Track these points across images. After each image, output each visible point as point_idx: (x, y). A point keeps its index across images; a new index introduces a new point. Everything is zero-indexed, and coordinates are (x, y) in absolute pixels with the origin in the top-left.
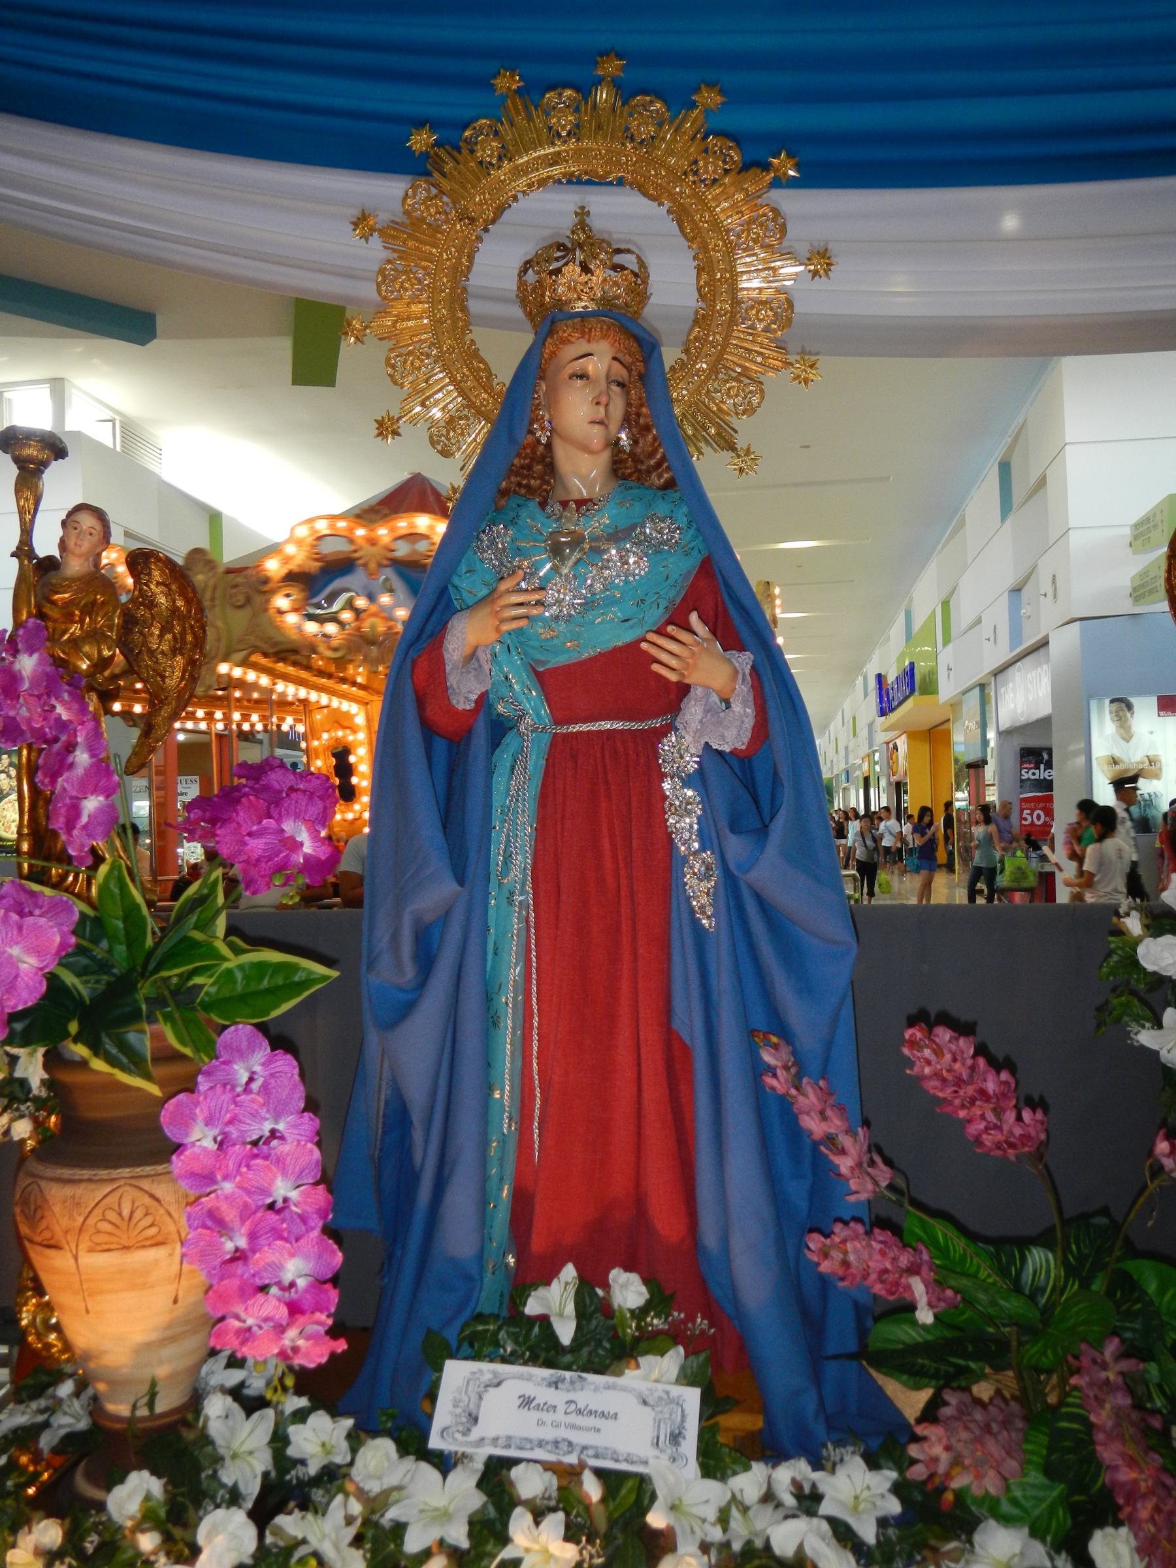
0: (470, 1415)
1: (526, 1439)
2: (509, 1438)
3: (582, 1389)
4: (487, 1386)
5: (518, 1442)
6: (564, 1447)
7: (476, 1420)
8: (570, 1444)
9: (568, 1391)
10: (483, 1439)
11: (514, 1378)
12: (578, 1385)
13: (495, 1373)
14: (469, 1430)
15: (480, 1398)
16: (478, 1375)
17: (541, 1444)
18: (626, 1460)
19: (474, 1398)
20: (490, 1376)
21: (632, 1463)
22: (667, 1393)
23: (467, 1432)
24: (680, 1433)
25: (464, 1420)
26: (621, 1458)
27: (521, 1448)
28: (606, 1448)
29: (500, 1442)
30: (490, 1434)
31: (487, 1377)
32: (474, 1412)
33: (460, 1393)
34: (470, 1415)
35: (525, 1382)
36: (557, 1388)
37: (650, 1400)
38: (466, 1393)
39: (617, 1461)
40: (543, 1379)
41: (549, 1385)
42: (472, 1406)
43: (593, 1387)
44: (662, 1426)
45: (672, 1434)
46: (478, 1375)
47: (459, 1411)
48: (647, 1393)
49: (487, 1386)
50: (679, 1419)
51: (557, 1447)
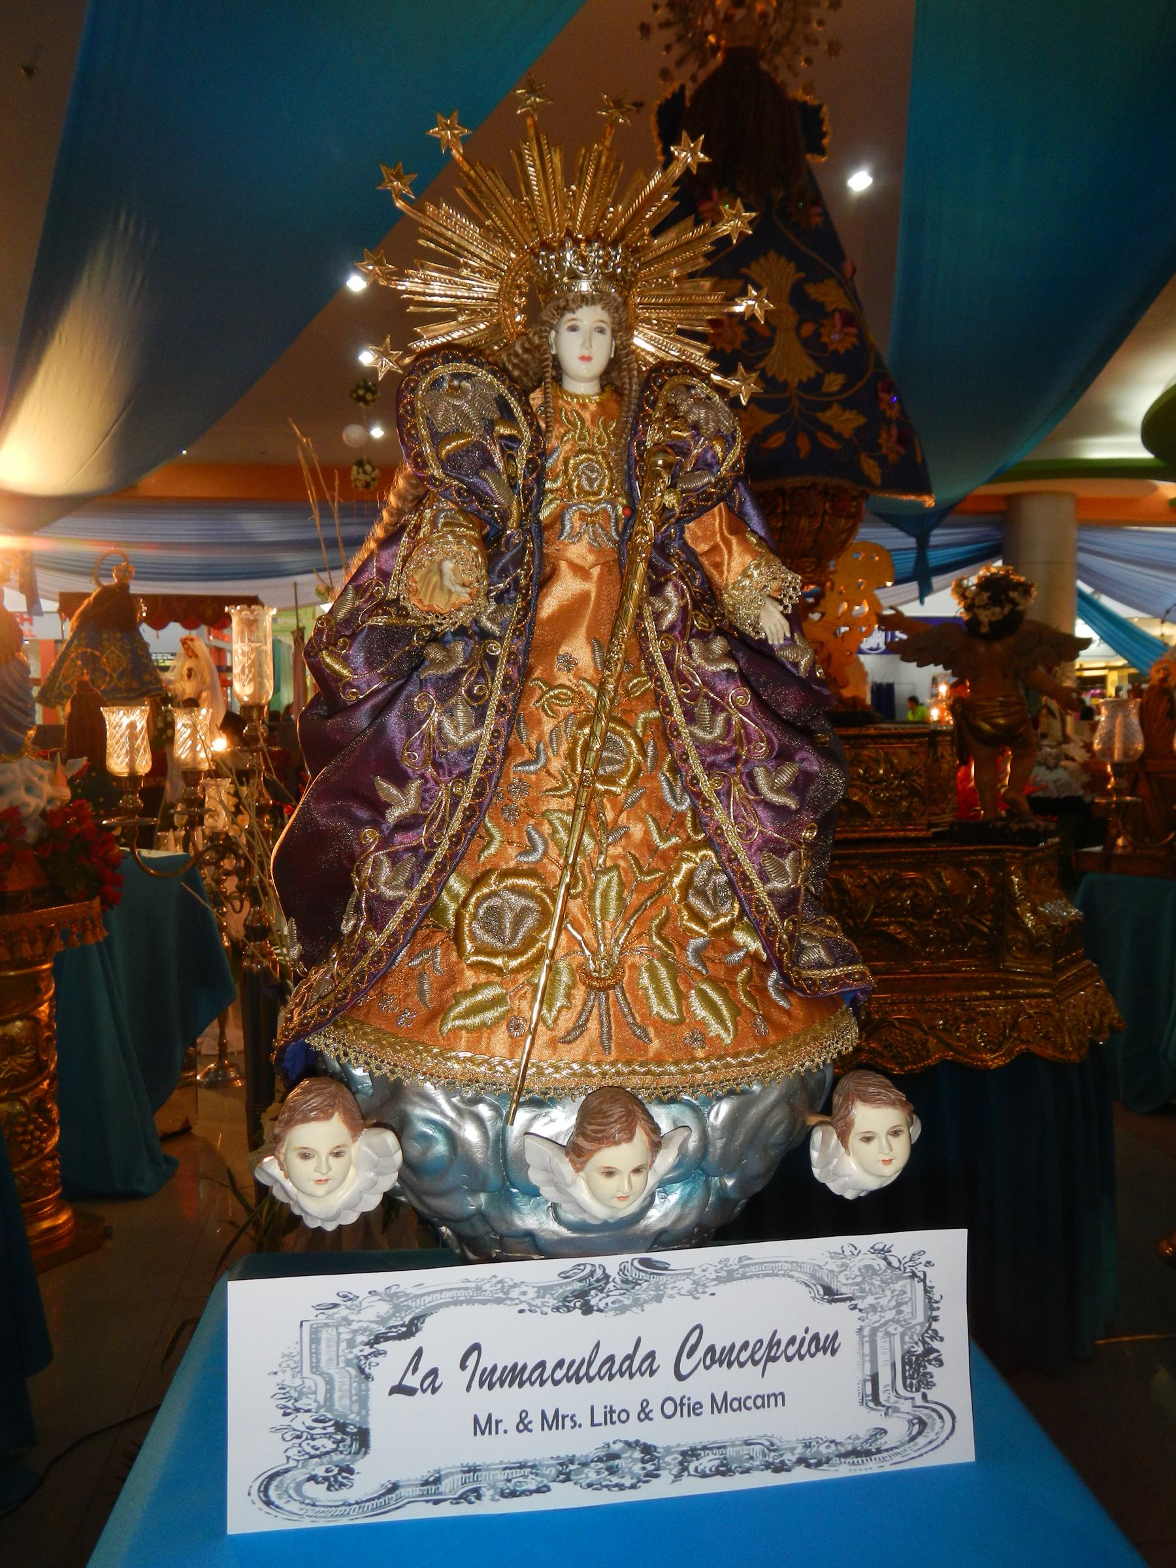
0: (340, 1427)
1: (522, 1466)
2: (473, 1470)
3: (658, 1299)
4: (378, 1339)
5: (502, 1476)
6: (631, 1463)
7: (363, 1438)
8: (647, 1449)
9: (623, 1309)
10: (395, 1487)
11: (456, 1303)
12: (644, 1291)
17: (566, 1470)
18: (803, 1461)
19: (344, 1378)
20: (384, 1308)
21: (819, 1464)
22: (884, 1252)
24: (929, 1351)
25: (330, 1445)
26: (789, 1458)
27: (513, 1494)
28: (747, 1443)
29: (445, 1487)
31: (372, 1313)
32: (352, 1416)
33: (298, 1370)
35: (490, 1307)
36: (587, 1309)
38: (315, 1368)
39: (780, 1468)
40: (543, 1291)
41: (564, 1305)
42: (343, 1405)
43: (687, 1285)
44: (882, 1343)
45: (906, 1361)
46: (342, 1312)
47: (302, 1421)
48: (833, 1265)
49: (378, 1339)
50: (920, 1317)
51: (612, 1471)
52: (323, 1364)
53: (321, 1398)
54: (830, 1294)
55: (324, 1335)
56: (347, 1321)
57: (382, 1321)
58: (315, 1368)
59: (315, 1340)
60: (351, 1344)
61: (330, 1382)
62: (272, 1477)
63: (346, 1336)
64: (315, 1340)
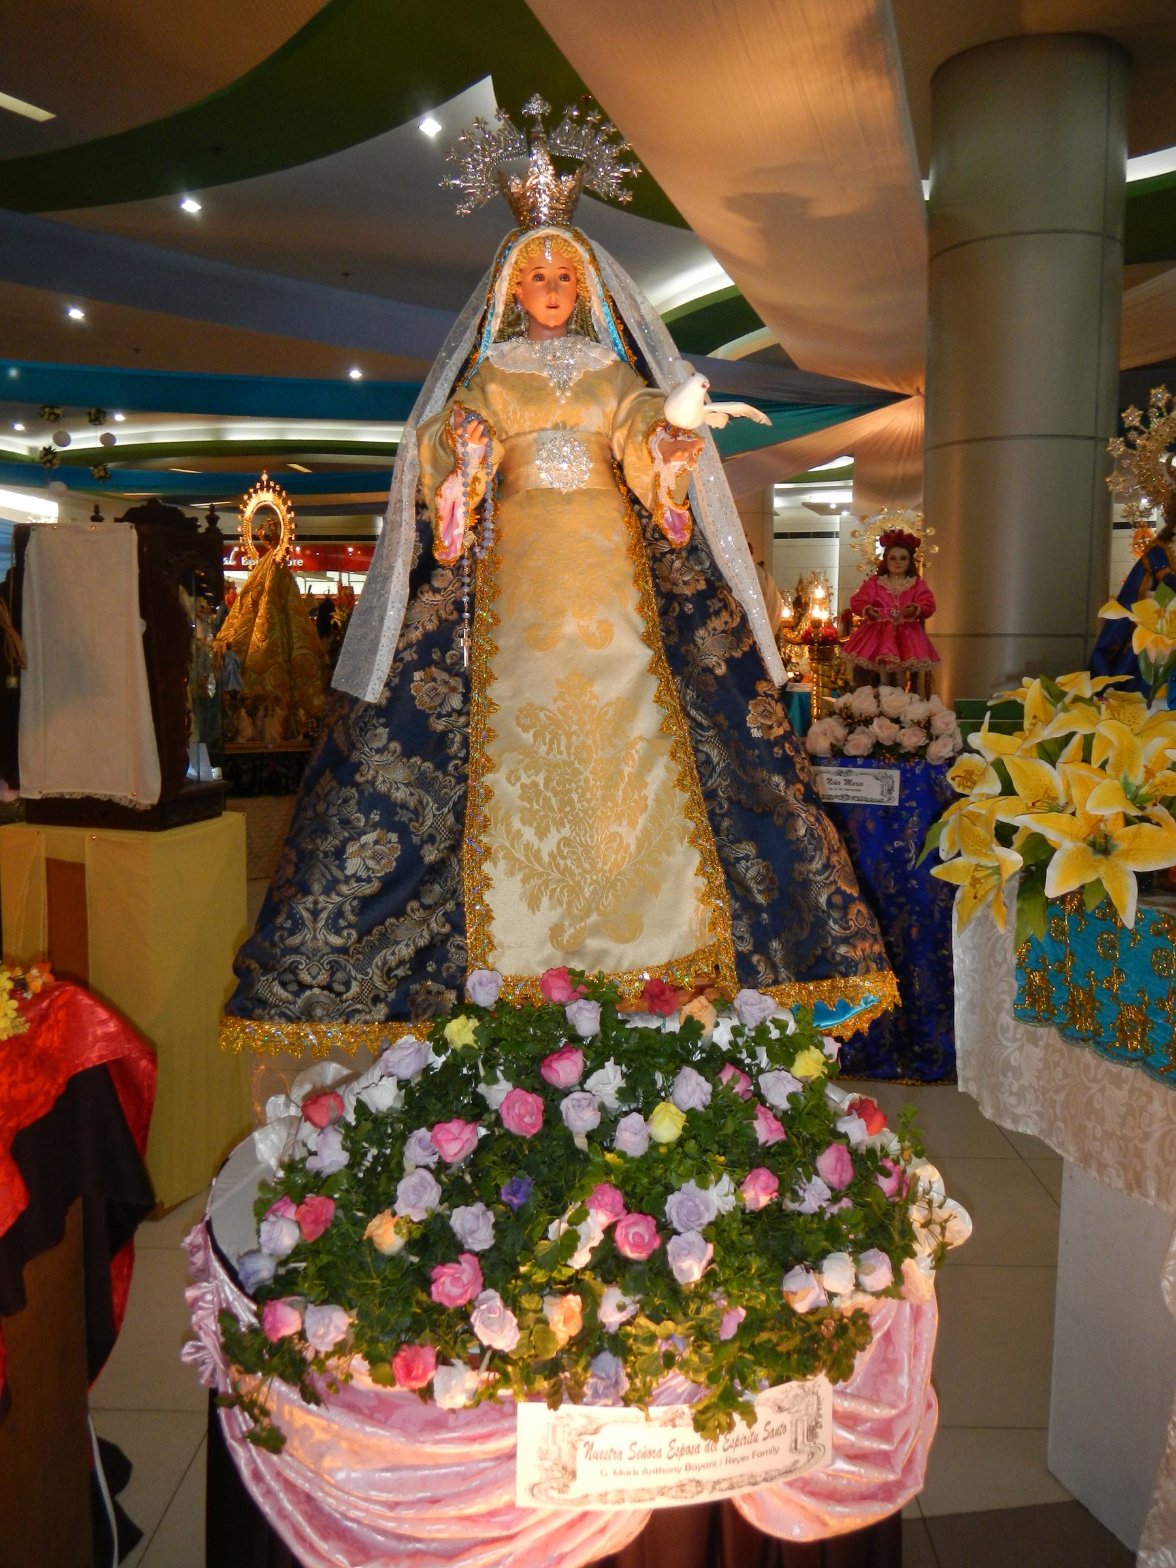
0: (564, 1468)
4: (581, 1434)
13: (590, 1419)
14: (566, 1486)
15: (574, 1448)
16: (566, 1420)
19: (566, 1448)
20: (584, 1421)
23: (564, 1489)
25: (558, 1475)
30: (595, 1490)
34: (564, 1468)
37: (786, 1405)
38: (554, 1442)
42: (565, 1458)
46: (566, 1420)
47: (548, 1464)
49: (581, 1434)
52: (558, 1441)
53: (556, 1454)
54: (780, 1409)
55: (559, 1430)
56: (568, 1425)
57: (584, 1427)
58: (554, 1442)
59: (554, 1431)
60: (570, 1434)
61: (560, 1449)
62: (534, 1485)
63: (567, 1430)
64: (554, 1431)
